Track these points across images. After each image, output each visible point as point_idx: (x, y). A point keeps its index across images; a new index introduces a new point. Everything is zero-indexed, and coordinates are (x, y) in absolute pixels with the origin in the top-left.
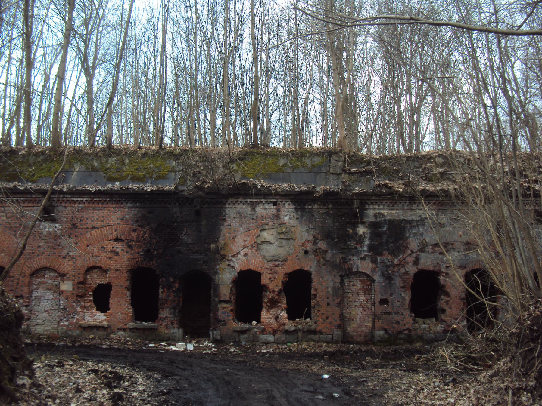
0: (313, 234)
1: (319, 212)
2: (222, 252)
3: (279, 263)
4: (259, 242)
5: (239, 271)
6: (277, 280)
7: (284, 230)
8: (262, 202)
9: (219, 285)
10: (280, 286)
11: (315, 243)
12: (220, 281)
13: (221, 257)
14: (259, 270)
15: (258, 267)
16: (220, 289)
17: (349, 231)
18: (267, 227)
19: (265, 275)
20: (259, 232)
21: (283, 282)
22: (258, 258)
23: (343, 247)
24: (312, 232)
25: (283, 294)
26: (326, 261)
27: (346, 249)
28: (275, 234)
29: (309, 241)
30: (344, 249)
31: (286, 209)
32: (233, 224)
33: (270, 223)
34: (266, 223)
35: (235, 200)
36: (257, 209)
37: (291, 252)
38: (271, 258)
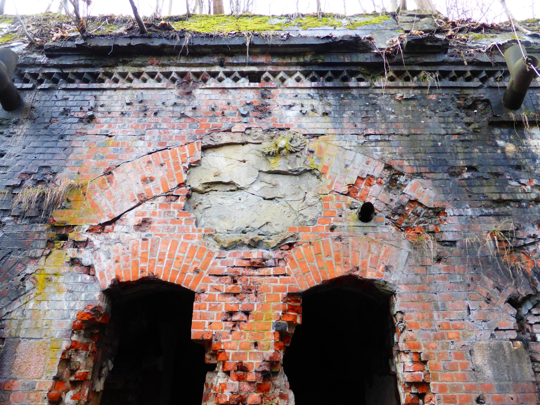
0: (382, 159)
1: (393, 96)
2: (59, 216)
3: (267, 253)
4: (196, 185)
5: (108, 283)
6: (258, 318)
7: (282, 143)
8: (214, 75)
9: (16, 340)
10: (270, 348)
11: (393, 183)
12: (26, 324)
13: (52, 234)
14: (188, 281)
15: (186, 268)
16: (18, 361)
17: (503, 149)
18: (226, 138)
19: (211, 298)
20: (198, 154)
21: (282, 334)
22: (187, 237)
23: (496, 197)
24: (378, 151)
25: (282, 380)
26: (442, 243)
27: (506, 202)
28: (252, 158)
29: (370, 177)
30: (500, 202)
31: (288, 91)
32: (116, 130)
33: (237, 127)
34: (225, 127)
35: (136, 70)
36: (197, 92)
37: (311, 214)
38: (236, 237)
